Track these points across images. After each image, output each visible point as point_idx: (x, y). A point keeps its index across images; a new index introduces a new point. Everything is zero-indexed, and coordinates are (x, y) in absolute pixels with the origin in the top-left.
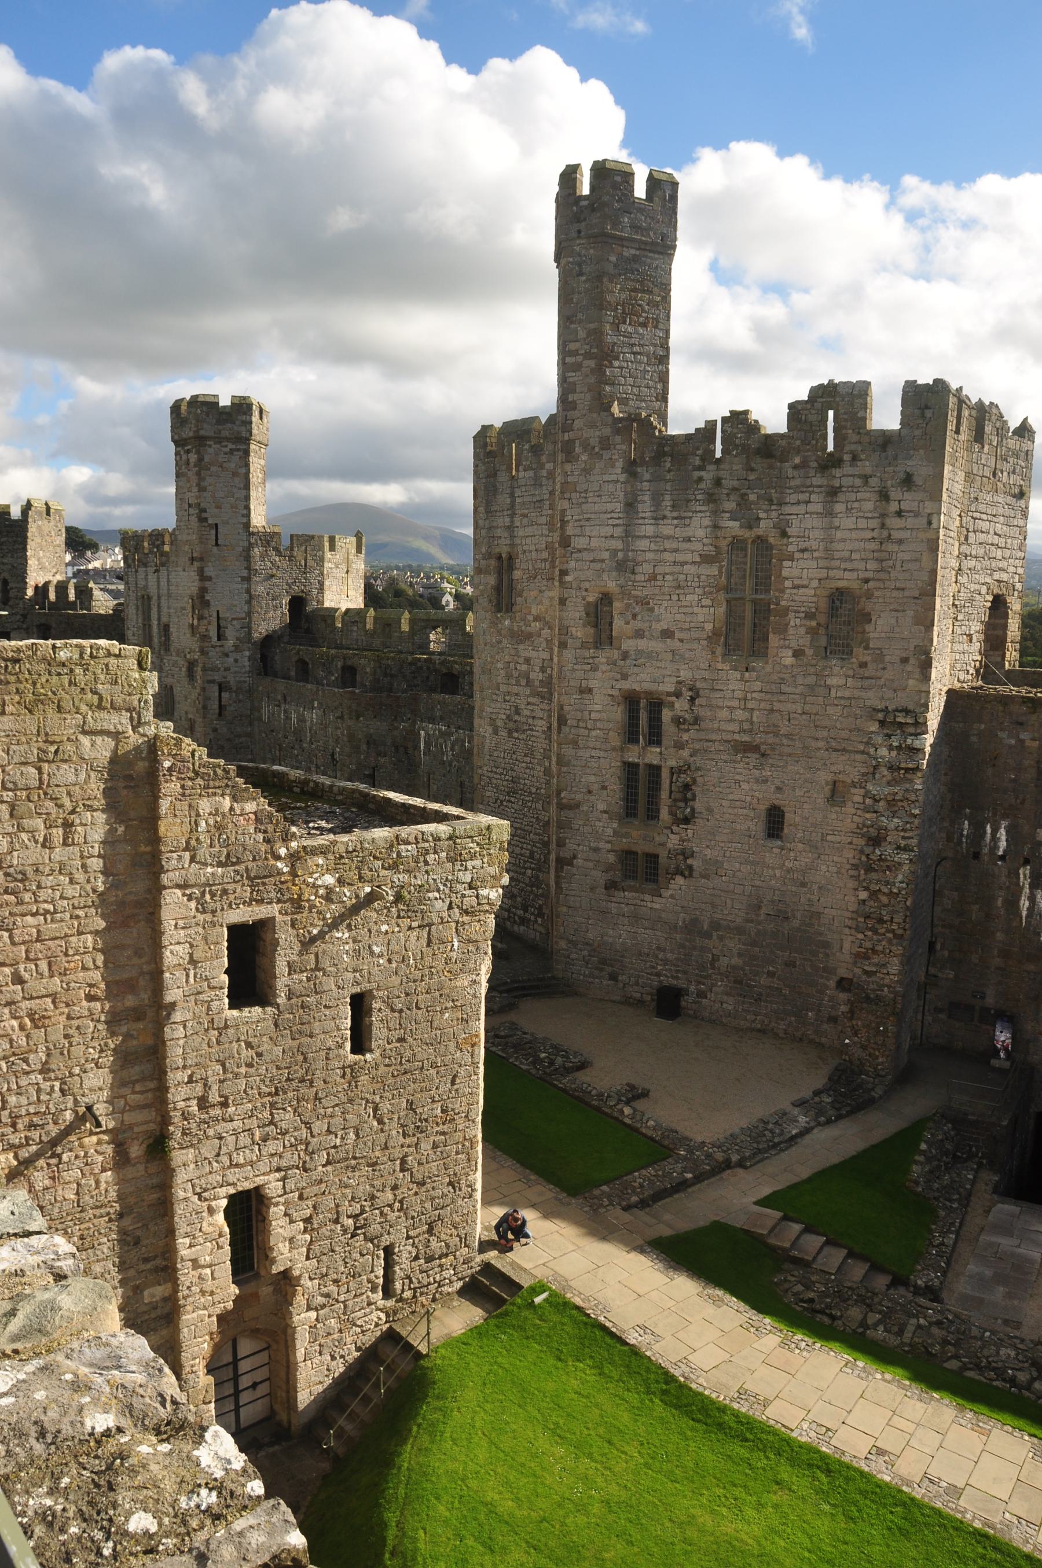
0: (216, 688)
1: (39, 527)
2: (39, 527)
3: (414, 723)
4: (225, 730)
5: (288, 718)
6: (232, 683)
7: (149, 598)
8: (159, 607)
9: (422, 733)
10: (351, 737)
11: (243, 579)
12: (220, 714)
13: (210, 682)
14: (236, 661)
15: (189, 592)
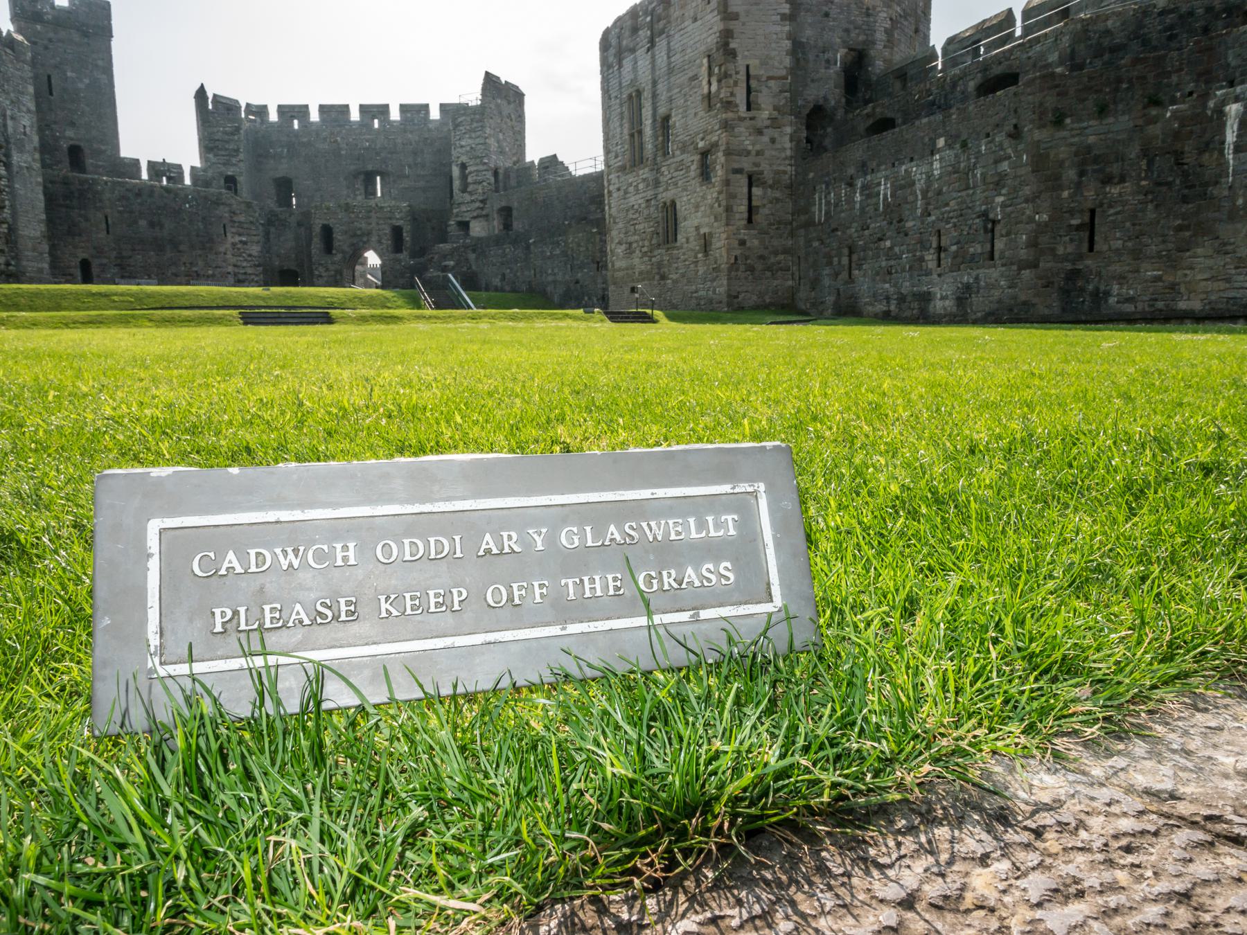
0: (745, 181)
1: (498, 106)
2: (498, 106)
3: (1205, 96)
4: (756, 242)
5: (870, 192)
6: (768, 176)
7: (639, 93)
8: (654, 96)
9: (1234, 109)
10: (1040, 161)
11: (784, 17)
12: (750, 220)
13: (738, 171)
14: (773, 141)
15: (703, 48)
